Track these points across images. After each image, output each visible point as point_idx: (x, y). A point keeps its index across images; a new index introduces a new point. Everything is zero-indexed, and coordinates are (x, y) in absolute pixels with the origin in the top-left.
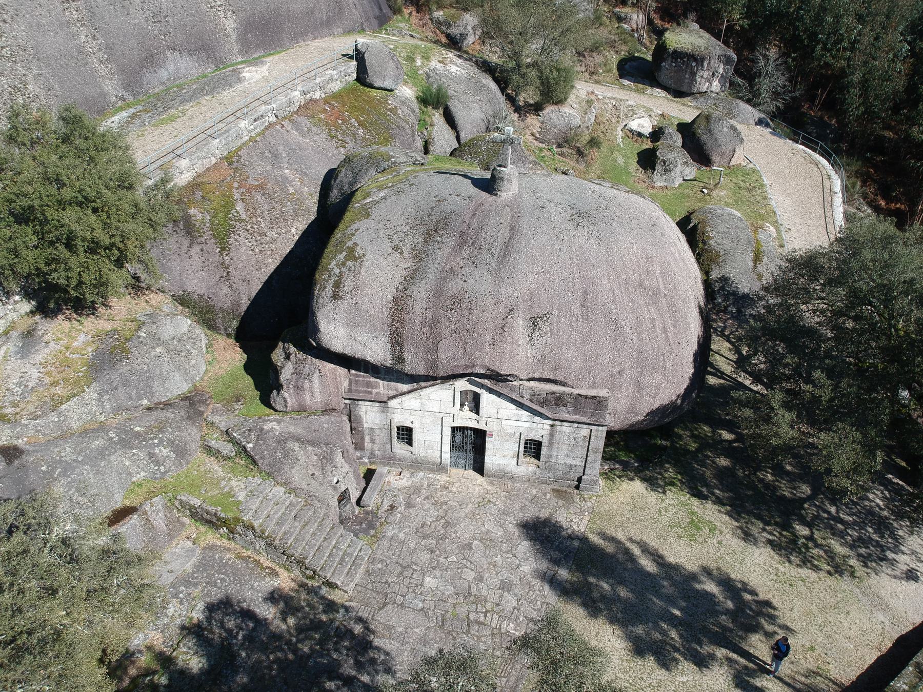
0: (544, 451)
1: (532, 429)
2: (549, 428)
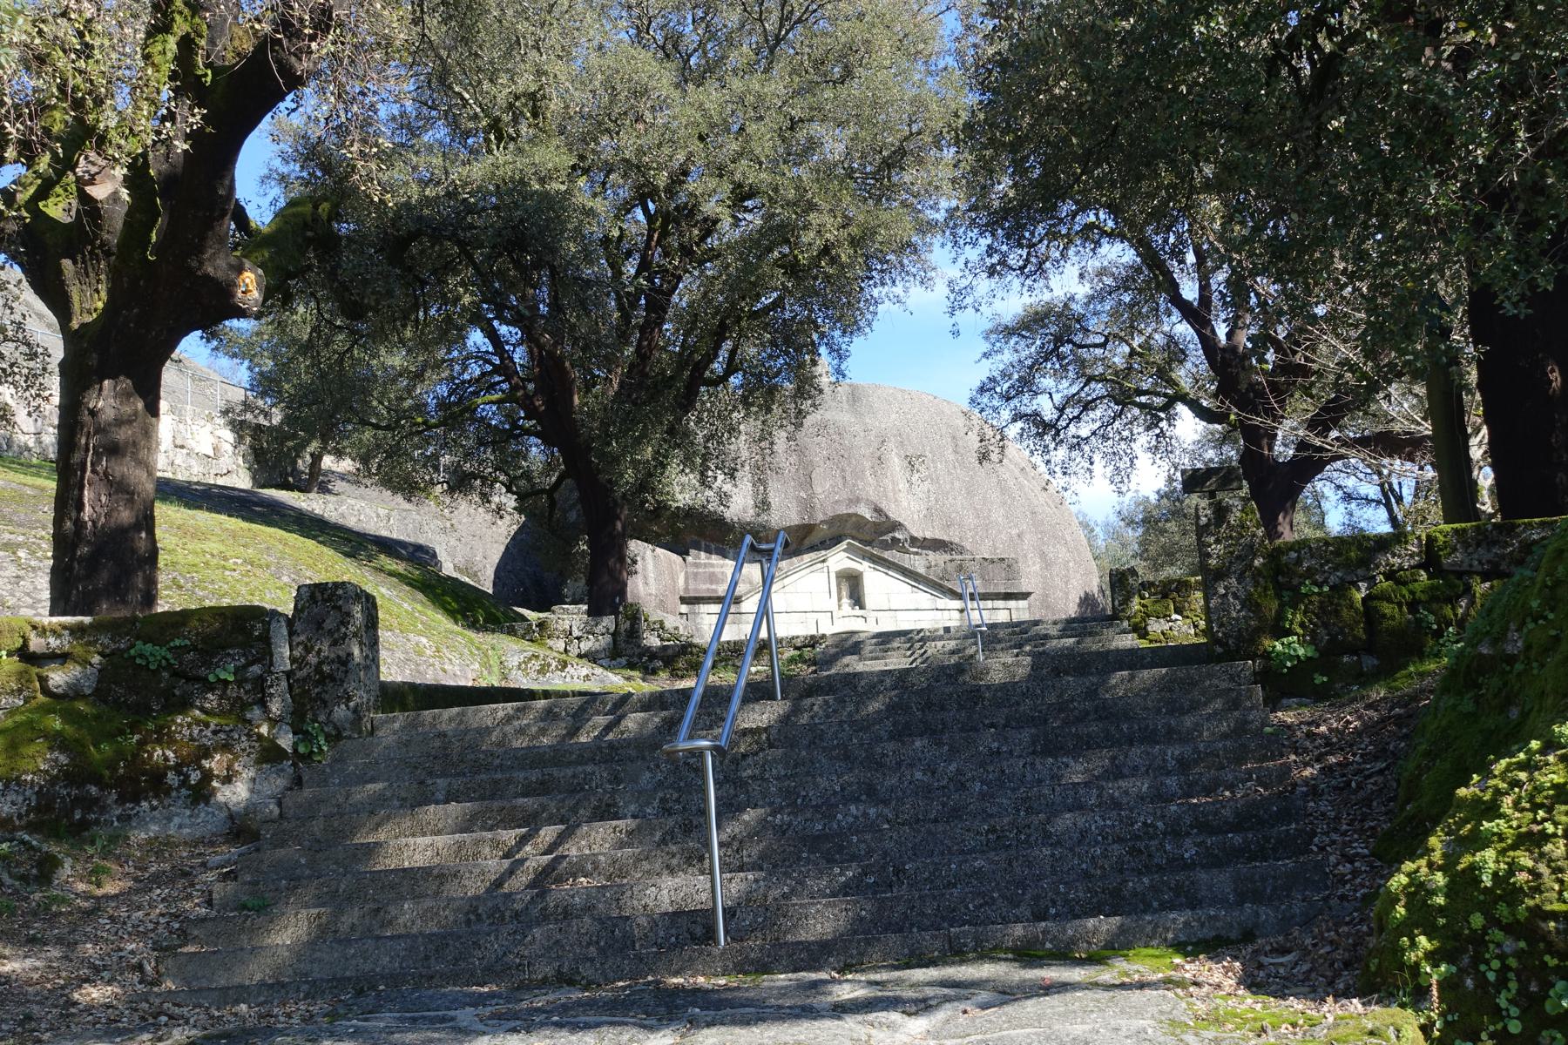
2: (956, 615)
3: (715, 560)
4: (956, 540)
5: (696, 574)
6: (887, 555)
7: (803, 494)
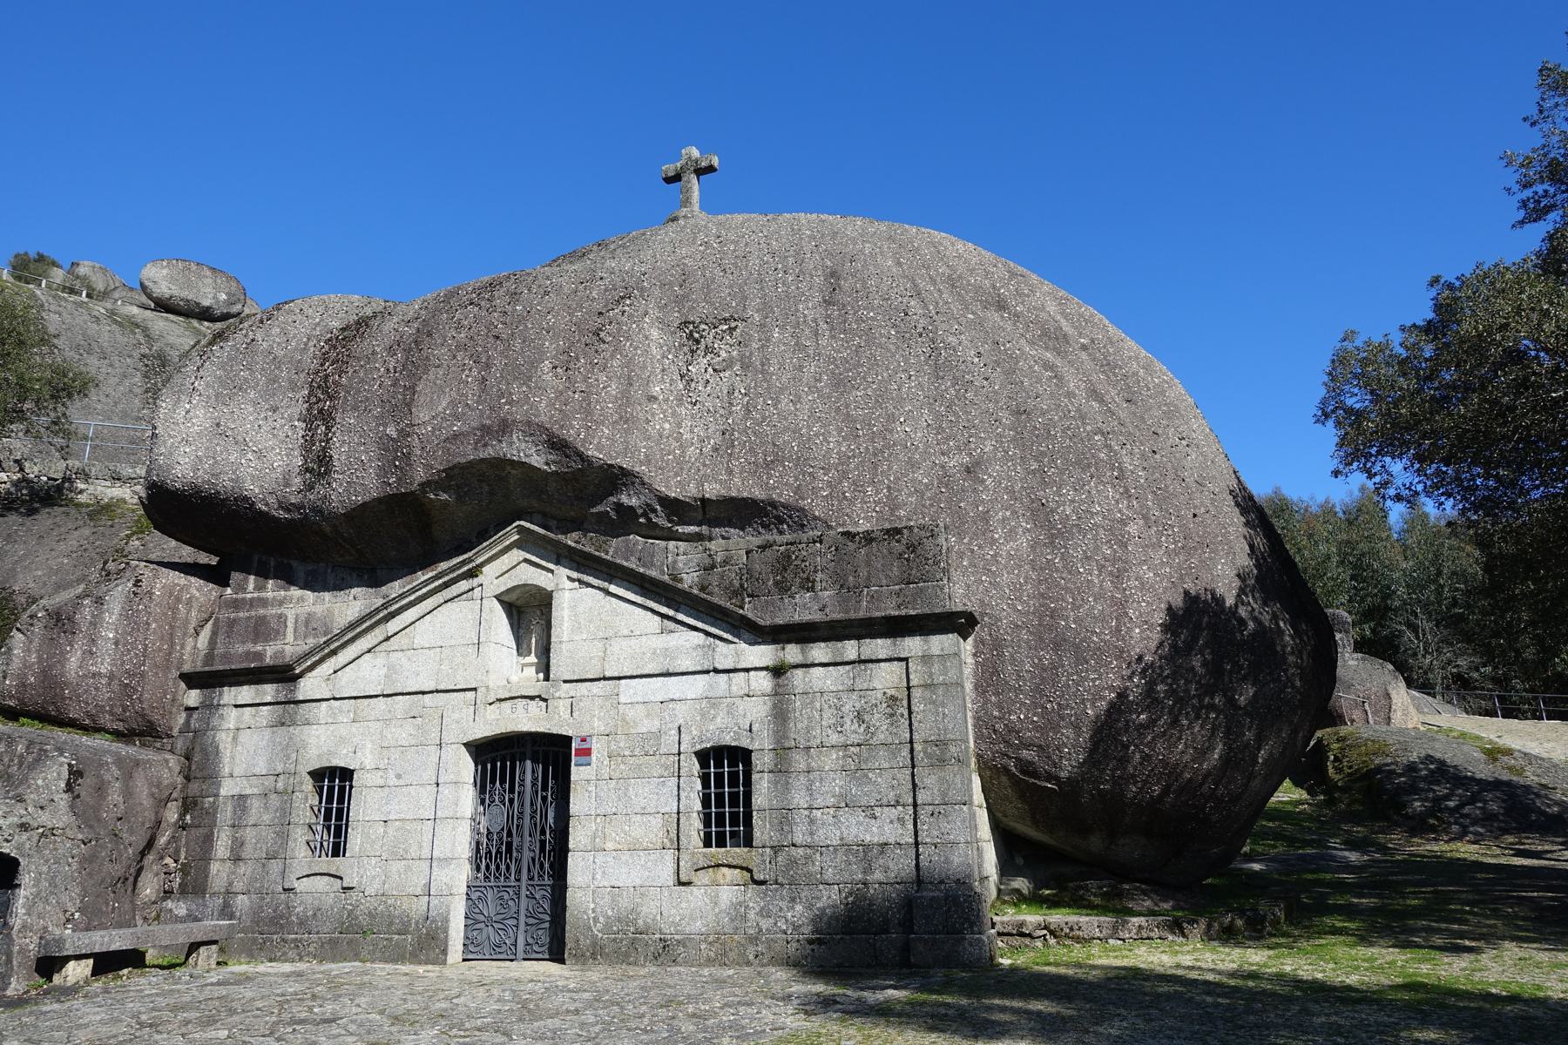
0: (763, 791)
1: (712, 701)
2: (763, 682)
3: (272, 590)
4: (785, 496)
5: (232, 623)
6: (613, 550)
7: (391, 431)
